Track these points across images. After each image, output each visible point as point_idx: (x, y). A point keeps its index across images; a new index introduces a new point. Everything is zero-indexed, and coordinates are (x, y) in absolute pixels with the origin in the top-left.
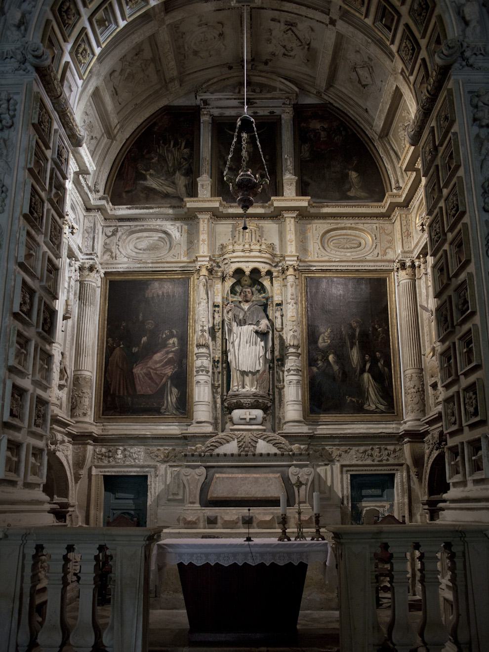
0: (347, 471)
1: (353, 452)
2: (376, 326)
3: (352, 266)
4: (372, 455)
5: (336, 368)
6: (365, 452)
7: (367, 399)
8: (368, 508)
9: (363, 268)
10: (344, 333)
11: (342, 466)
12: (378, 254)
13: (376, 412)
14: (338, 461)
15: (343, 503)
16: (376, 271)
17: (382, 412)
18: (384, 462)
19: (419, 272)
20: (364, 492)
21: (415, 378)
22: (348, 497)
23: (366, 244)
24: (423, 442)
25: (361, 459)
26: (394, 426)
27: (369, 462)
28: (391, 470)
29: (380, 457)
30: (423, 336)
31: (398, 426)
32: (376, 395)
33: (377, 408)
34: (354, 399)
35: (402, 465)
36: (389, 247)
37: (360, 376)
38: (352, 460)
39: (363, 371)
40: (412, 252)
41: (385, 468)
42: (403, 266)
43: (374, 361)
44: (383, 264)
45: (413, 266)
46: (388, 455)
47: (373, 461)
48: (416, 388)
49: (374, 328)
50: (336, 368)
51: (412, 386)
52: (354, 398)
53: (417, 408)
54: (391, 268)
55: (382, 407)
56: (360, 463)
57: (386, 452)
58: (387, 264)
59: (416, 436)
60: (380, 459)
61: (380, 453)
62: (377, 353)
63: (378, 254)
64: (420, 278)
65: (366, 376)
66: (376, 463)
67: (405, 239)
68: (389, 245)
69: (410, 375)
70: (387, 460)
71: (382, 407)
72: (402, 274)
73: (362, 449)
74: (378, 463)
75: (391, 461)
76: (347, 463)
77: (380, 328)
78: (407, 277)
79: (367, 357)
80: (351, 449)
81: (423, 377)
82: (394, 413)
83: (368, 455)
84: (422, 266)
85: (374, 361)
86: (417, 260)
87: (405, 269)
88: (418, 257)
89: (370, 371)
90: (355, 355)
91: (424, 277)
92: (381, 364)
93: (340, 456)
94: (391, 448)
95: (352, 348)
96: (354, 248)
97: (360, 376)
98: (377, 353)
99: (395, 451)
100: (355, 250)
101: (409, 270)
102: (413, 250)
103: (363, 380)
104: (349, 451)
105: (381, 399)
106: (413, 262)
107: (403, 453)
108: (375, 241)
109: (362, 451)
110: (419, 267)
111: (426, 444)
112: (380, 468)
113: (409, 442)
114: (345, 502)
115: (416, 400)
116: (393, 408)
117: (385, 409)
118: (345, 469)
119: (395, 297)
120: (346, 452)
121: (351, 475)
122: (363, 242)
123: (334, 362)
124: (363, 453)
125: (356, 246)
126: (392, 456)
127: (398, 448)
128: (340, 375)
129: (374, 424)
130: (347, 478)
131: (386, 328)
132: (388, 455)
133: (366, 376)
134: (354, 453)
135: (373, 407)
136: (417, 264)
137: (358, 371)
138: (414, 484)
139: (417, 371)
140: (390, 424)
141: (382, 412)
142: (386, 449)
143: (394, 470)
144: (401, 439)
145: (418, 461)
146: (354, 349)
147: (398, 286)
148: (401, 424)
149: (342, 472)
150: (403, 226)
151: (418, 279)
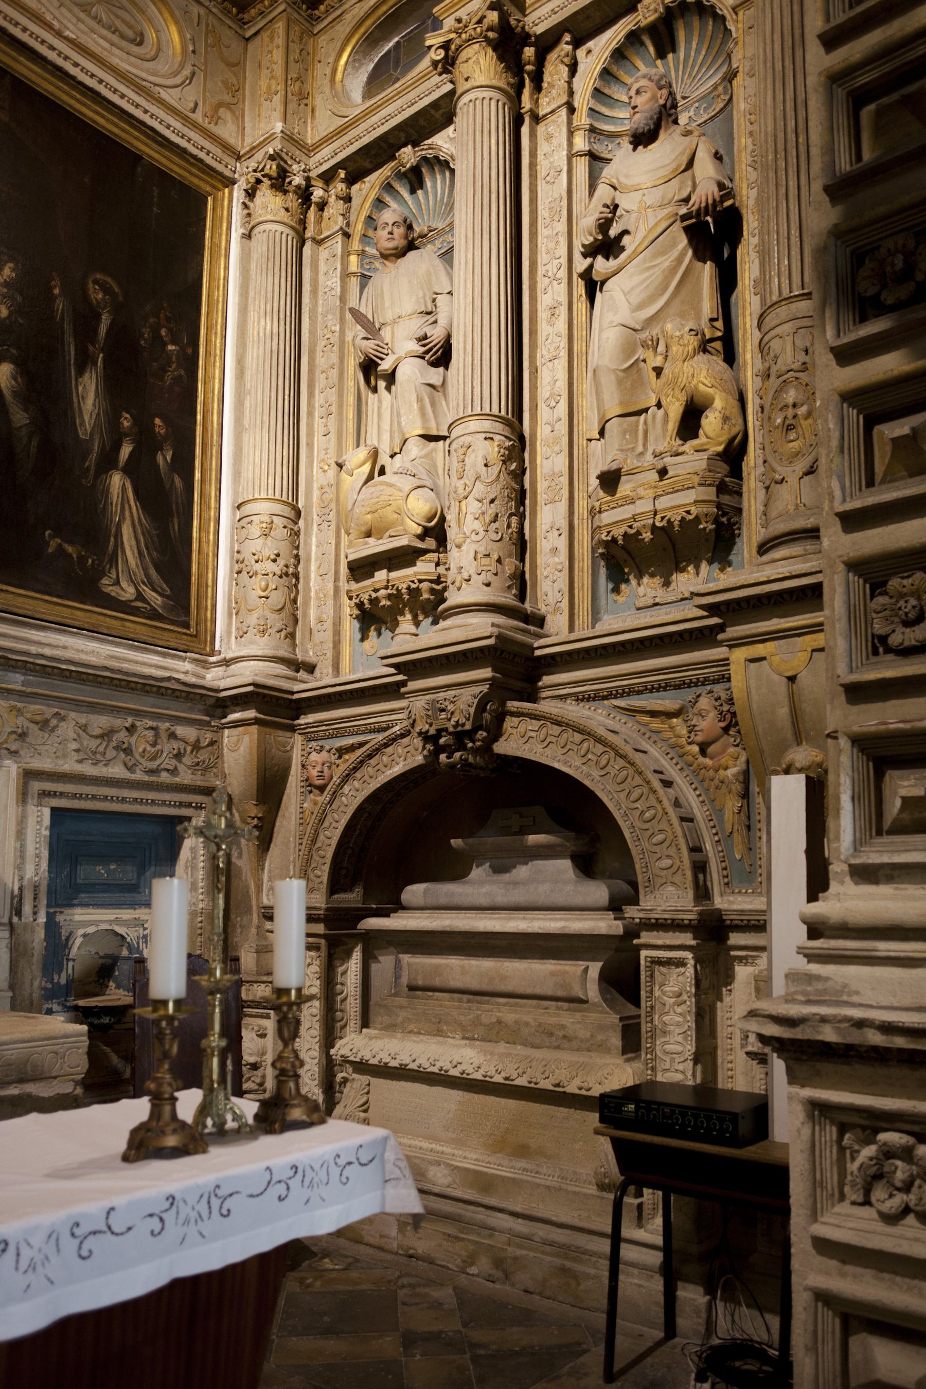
0: (45, 794)
1: (67, 729)
2: (163, 332)
3: (115, 91)
4: (128, 751)
5: (20, 417)
6: (106, 735)
7: (113, 560)
8: (91, 930)
9: (146, 118)
10: (60, 305)
11: (29, 775)
12: (196, 105)
13: (135, 611)
14: (14, 753)
15: (19, 913)
16: (183, 153)
17: (154, 615)
18: (165, 777)
19: (319, 220)
20: (84, 872)
21: (280, 533)
22: (36, 887)
23: (159, 50)
24: (292, 729)
25: (95, 757)
26: (188, 666)
27: (117, 771)
28: (181, 805)
29: (154, 758)
30: (310, 414)
31: (200, 671)
32: (140, 553)
33: (140, 597)
34: (70, 549)
35: (208, 791)
36: (228, 106)
37: (96, 477)
38: (65, 756)
39: (108, 462)
40: (309, 150)
41: (167, 796)
42: (280, 182)
43: (147, 445)
44: (207, 144)
45: (305, 194)
46: (178, 756)
47: (130, 769)
48: (281, 562)
49: (156, 337)
50: (20, 417)
51: (269, 552)
52: (71, 543)
53: (279, 625)
54: (227, 173)
55: (156, 599)
56: (88, 769)
57: (175, 745)
58: (218, 152)
59: (276, 708)
60: (153, 765)
61: (154, 745)
62: (158, 421)
63: (196, 105)
64: (319, 242)
65: (117, 480)
66: (139, 776)
67: (292, 106)
68: (227, 98)
69: (267, 519)
70: (174, 772)
71: (156, 599)
72: (269, 203)
73: (101, 722)
74: (146, 778)
75: (186, 777)
76: (45, 764)
77: (173, 343)
78: (283, 216)
79: (126, 422)
80: (63, 719)
81: (297, 534)
82: (187, 626)
83: (116, 748)
84: (335, 208)
85: (147, 445)
86: (320, 184)
87: (285, 192)
88: (328, 177)
89: (129, 470)
90: (88, 394)
91: (338, 243)
92: (164, 458)
93: (23, 736)
94: (187, 732)
95: (80, 371)
96: (123, 37)
97: (96, 477)
98: (158, 421)
99: (196, 746)
100: (124, 44)
101: (293, 201)
102: (317, 147)
103: (106, 492)
104: (54, 722)
105: (153, 572)
106: (309, 186)
107: (220, 756)
108: (192, 59)
109: (98, 731)
110: (322, 206)
111: (298, 739)
112: (151, 795)
113: (257, 721)
114: (27, 909)
115: (278, 598)
116: (187, 609)
117: (164, 606)
118: (36, 786)
119: (227, 268)
120: (44, 725)
121: (54, 810)
122: (151, 36)
123: (15, 394)
124: (102, 736)
125: (130, 33)
126: (187, 760)
127: (208, 736)
128: (33, 450)
129: (131, 647)
130: (39, 820)
131: (189, 351)
132: (178, 756)
133: (117, 480)
134: (72, 735)
135: (127, 592)
136: (318, 193)
137: (94, 456)
138: (240, 856)
139: (287, 511)
140: (174, 657)
141: (154, 615)
142: (173, 736)
143: (189, 805)
144: (219, 711)
145: (270, 785)
146: (87, 375)
147: (248, 236)
148: (206, 665)
149: (23, 796)
150: (291, 58)
151: (313, 239)
